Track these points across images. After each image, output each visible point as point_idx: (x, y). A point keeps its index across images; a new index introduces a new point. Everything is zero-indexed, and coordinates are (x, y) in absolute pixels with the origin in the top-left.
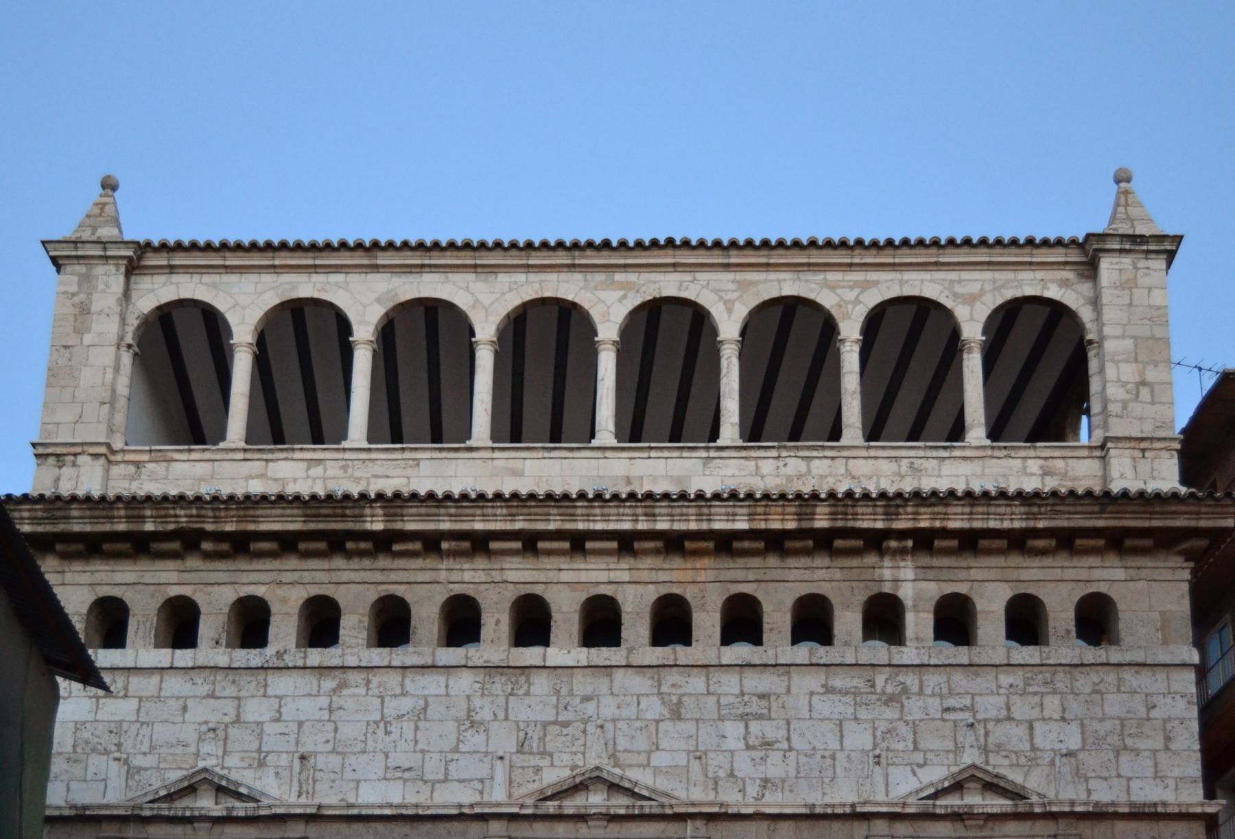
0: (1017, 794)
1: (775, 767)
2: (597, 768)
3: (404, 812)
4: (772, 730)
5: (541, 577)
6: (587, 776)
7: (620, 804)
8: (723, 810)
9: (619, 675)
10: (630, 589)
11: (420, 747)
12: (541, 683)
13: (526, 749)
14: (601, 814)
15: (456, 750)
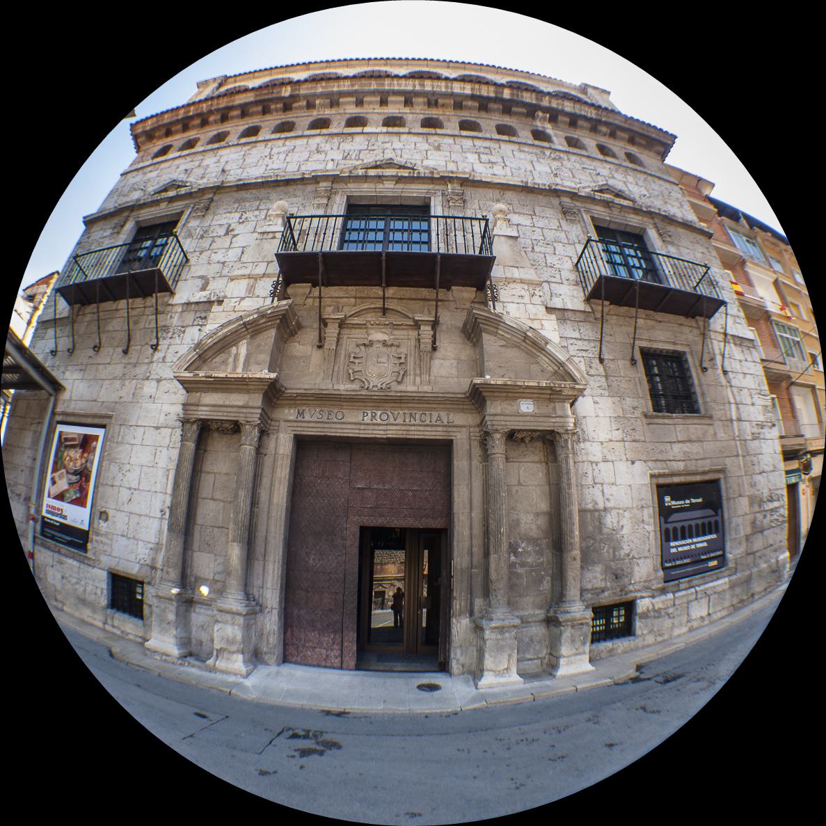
0: (633, 201)
1: (498, 170)
2: (391, 159)
3: (269, 179)
4: (493, 159)
5: (365, 111)
6: (384, 162)
7: (405, 173)
8: (471, 178)
9: (404, 137)
10: (411, 116)
11: (287, 160)
12: (358, 139)
13: (348, 157)
14: (392, 176)
15: (307, 160)
